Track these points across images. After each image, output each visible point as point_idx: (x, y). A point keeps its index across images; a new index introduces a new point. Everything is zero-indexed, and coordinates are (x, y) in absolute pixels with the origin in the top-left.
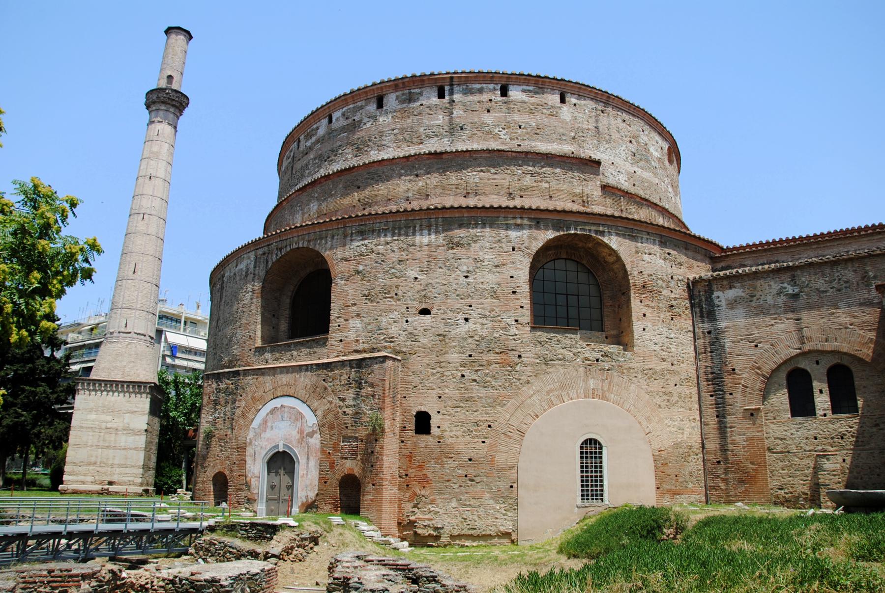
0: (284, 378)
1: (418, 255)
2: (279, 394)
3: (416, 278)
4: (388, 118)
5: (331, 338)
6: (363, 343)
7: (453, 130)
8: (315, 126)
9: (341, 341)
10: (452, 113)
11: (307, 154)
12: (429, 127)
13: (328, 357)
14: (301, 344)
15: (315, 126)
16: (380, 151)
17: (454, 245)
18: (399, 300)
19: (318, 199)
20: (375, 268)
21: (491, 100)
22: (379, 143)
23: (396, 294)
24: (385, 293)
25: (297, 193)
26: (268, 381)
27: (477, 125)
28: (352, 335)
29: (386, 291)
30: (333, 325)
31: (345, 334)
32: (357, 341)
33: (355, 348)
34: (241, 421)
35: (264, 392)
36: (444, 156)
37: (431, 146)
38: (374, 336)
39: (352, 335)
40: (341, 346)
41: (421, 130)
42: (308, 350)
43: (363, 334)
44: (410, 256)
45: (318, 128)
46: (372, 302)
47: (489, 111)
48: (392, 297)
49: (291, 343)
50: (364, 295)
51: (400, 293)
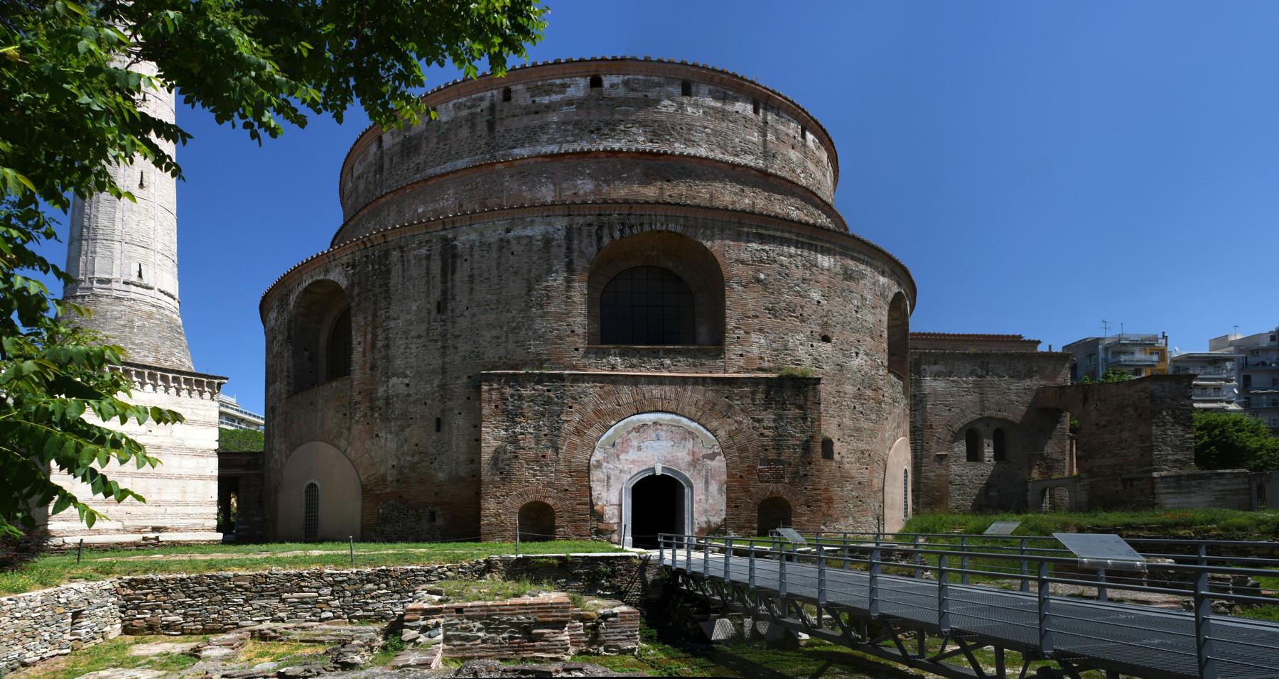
0: (656, 391)
1: (821, 278)
2: (647, 409)
3: (819, 302)
4: (698, 112)
5: (728, 350)
6: (769, 361)
7: (767, 154)
8: (558, 82)
9: (741, 355)
10: (766, 136)
11: (537, 113)
12: (744, 140)
13: (725, 371)
14: (679, 352)
15: (558, 82)
16: (688, 146)
17: (848, 276)
18: (804, 322)
19: (593, 177)
20: (779, 280)
21: (795, 137)
22: (687, 136)
23: (801, 315)
24: (790, 311)
25: (540, 160)
26: (626, 394)
27: (786, 158)
28: (755, 351)
29: (790, 309)
30: (730, 336)
31: (747, 349)
32: (762, 358)
33: (759, 366)
34: (577, 440)
35: (619, 405)
36: (771, 179)
37: (748, 160)
38: (781, 356)
39: (755, 351)
40: (742, 362)
41: (737, 140)
42: (690, 360)
43: (768, 352)
44: (812, 277)
45: (565, 86)
46: (776, 317)
47: (793, 148)
48: (797, 317)
49: (659, 350)
50: (767, 309)
51: (805, 314)
